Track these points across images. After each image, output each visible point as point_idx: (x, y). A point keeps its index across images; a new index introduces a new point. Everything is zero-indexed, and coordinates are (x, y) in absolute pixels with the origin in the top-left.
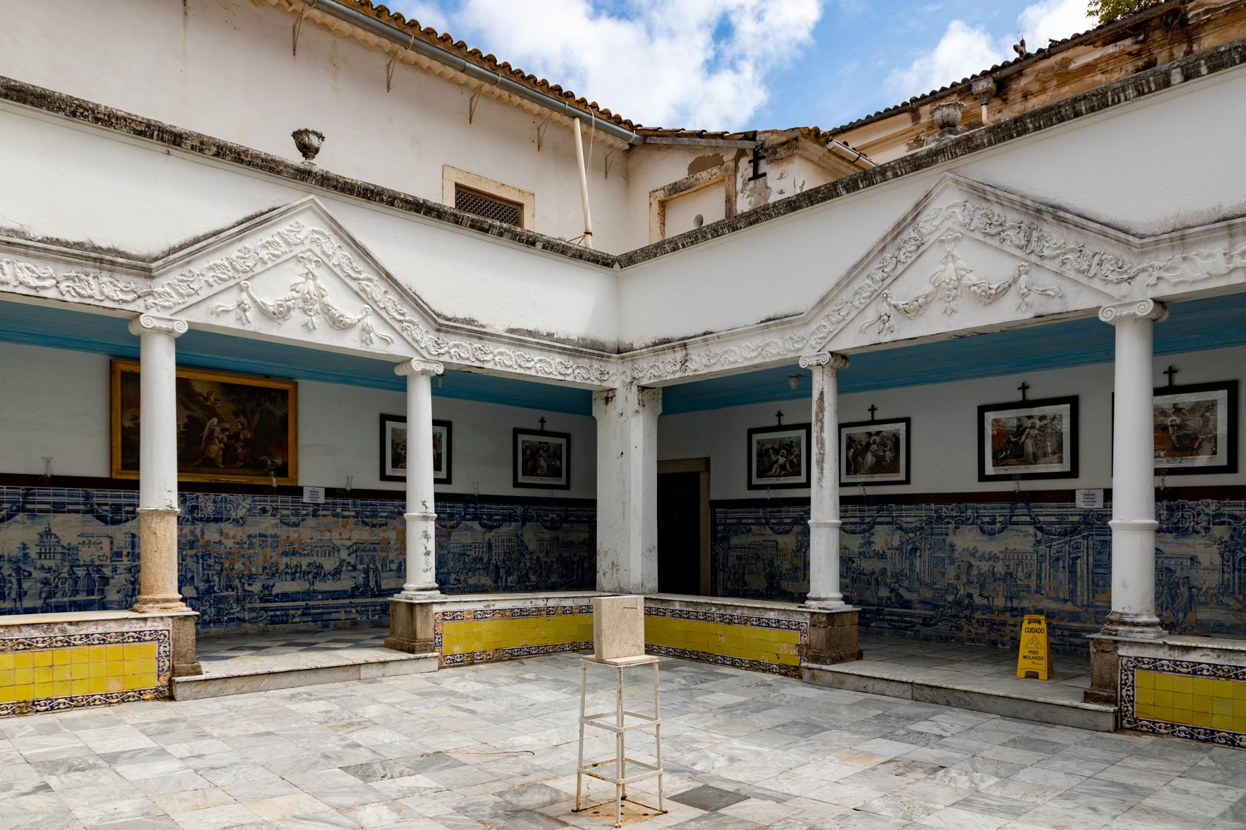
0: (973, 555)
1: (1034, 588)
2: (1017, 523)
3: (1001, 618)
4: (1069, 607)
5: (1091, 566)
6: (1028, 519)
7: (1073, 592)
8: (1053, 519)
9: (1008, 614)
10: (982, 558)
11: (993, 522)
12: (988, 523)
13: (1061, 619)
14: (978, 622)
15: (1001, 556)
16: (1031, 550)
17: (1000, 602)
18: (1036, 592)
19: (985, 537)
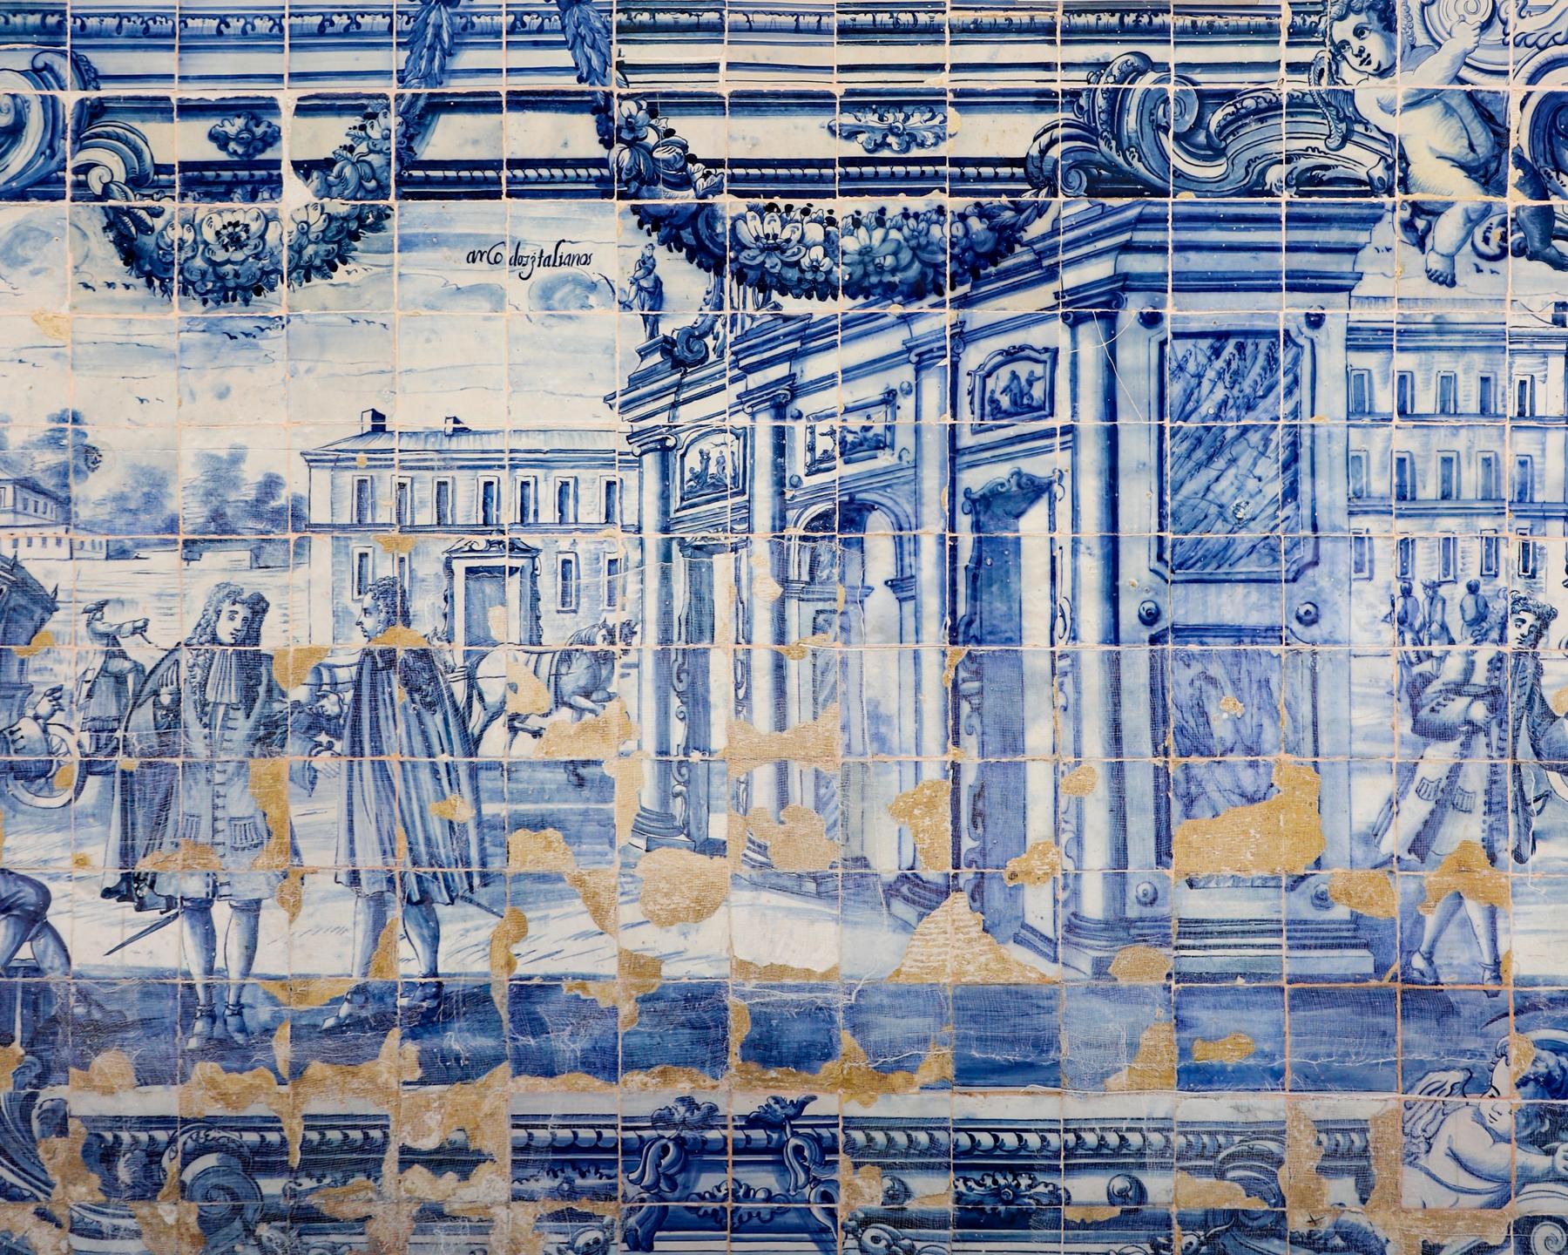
0: (49, 495)
1: (637, 786)
2: (474, 181)
3: (333, 1095)
4: (951, 949)
5: (1136, 565)
6: (577, 136)
7: (983, 808)
8: (803, 136)
9: (397, 1055)
10: (143, 523)
11: (246, 170)
12: (200, 180)
13: (891, 1065)
14: (102, 1154)
15: (325, 498)
16: (612, 430)
17: (318, 944)
18: (656, 828)
19: (171, 319)
